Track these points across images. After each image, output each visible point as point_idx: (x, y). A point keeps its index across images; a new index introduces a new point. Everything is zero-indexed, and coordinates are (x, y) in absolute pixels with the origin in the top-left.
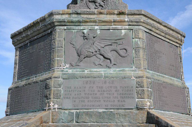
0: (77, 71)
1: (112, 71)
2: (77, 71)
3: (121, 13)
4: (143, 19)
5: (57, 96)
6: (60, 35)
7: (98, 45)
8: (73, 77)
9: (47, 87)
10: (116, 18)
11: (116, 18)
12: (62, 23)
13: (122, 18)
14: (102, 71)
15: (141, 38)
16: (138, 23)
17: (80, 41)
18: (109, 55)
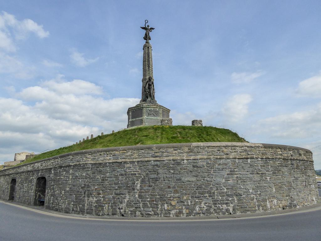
0: (148, 118)
1: (155, 118)
2: (148, 118)
3: (157, 106)
4: (162, 107)
5: (145, 122)
6: (144, 110)
7: (152, 112)
8: (148, 119)
9: (142, 120)
10: (156, 107)
11: (156, 107)
12: (145, 107)
13: (157, 107)
14: (153, 118)
15: (161, 112)
16: (160, 108)
17: (149, 111)
18: (155, 115)
